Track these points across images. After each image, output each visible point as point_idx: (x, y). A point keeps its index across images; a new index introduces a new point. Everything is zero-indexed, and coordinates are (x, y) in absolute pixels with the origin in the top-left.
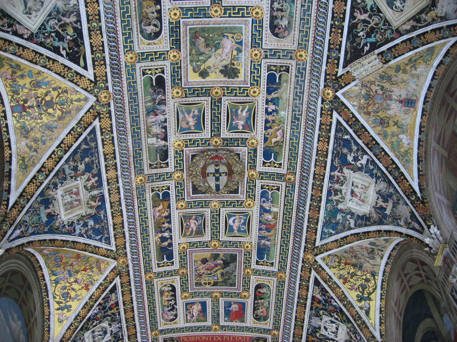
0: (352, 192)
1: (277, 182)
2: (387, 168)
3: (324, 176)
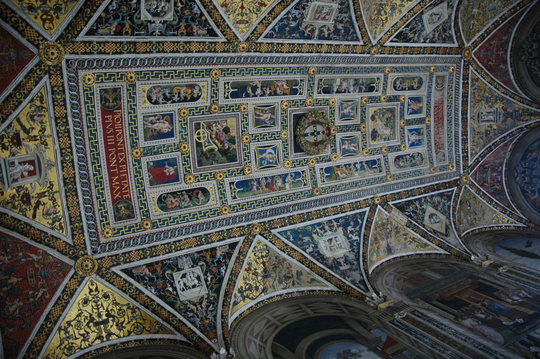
0: (330, 240)
1: (310, 183)
2: (363, 253)
3: (329, 215)
